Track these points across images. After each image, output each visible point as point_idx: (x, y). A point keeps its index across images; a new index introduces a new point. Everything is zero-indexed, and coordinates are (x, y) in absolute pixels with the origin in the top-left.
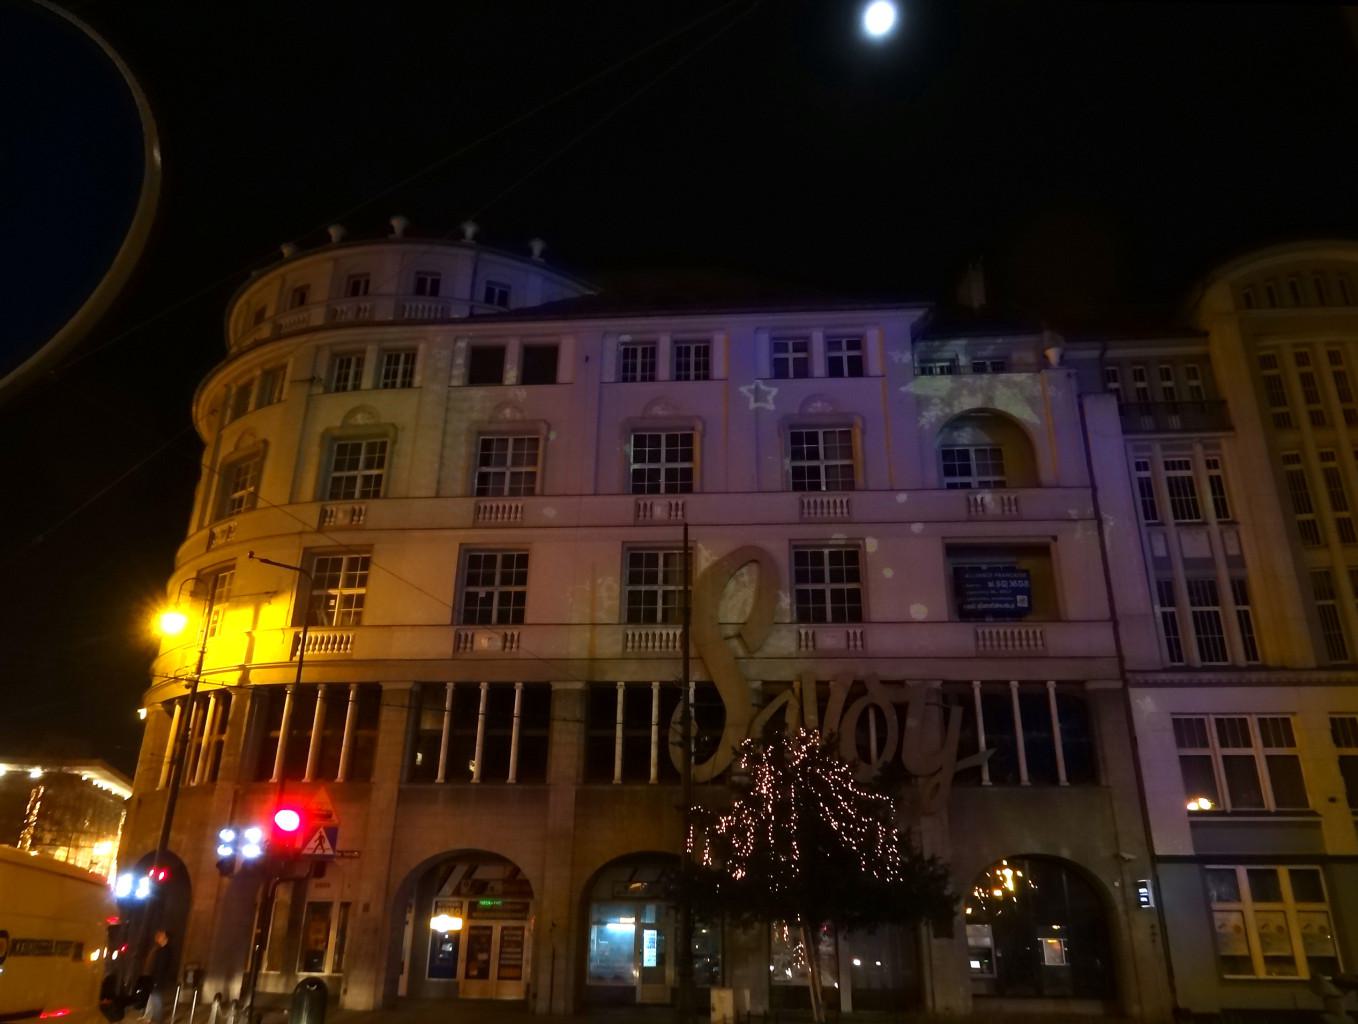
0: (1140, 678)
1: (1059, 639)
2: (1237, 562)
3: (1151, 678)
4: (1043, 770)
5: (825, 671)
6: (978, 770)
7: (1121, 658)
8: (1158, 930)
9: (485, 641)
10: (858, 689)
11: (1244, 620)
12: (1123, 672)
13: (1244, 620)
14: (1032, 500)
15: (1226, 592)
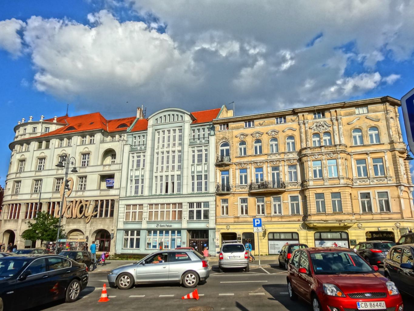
0: (122, 198)
1: (112, 192)
2: (143, 176)
3: (122, 198)
4: (106, 215)
5: (77, 199)
6: (97, 213)
7: (119, 195)
8: (115, 241)
9: (35, 196)
10: (81, 202)
11: (142, 186)
12: (120, 198)
13: (142, 186)
14: (114, 167)
15: (140, 181)
